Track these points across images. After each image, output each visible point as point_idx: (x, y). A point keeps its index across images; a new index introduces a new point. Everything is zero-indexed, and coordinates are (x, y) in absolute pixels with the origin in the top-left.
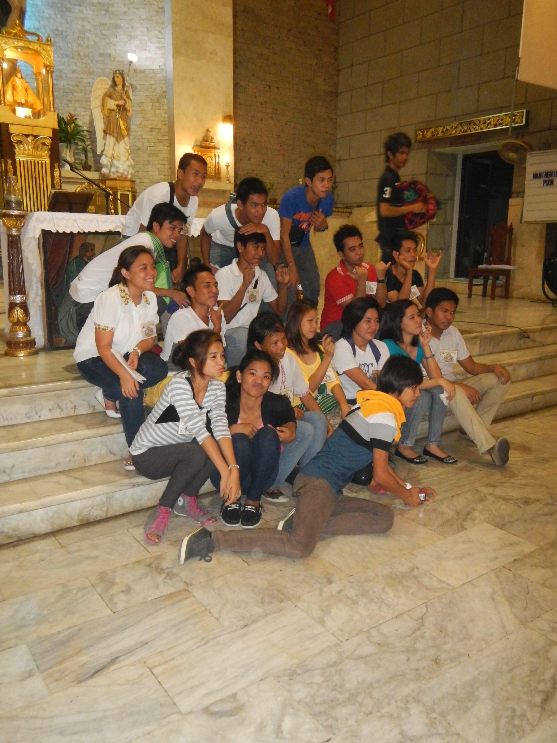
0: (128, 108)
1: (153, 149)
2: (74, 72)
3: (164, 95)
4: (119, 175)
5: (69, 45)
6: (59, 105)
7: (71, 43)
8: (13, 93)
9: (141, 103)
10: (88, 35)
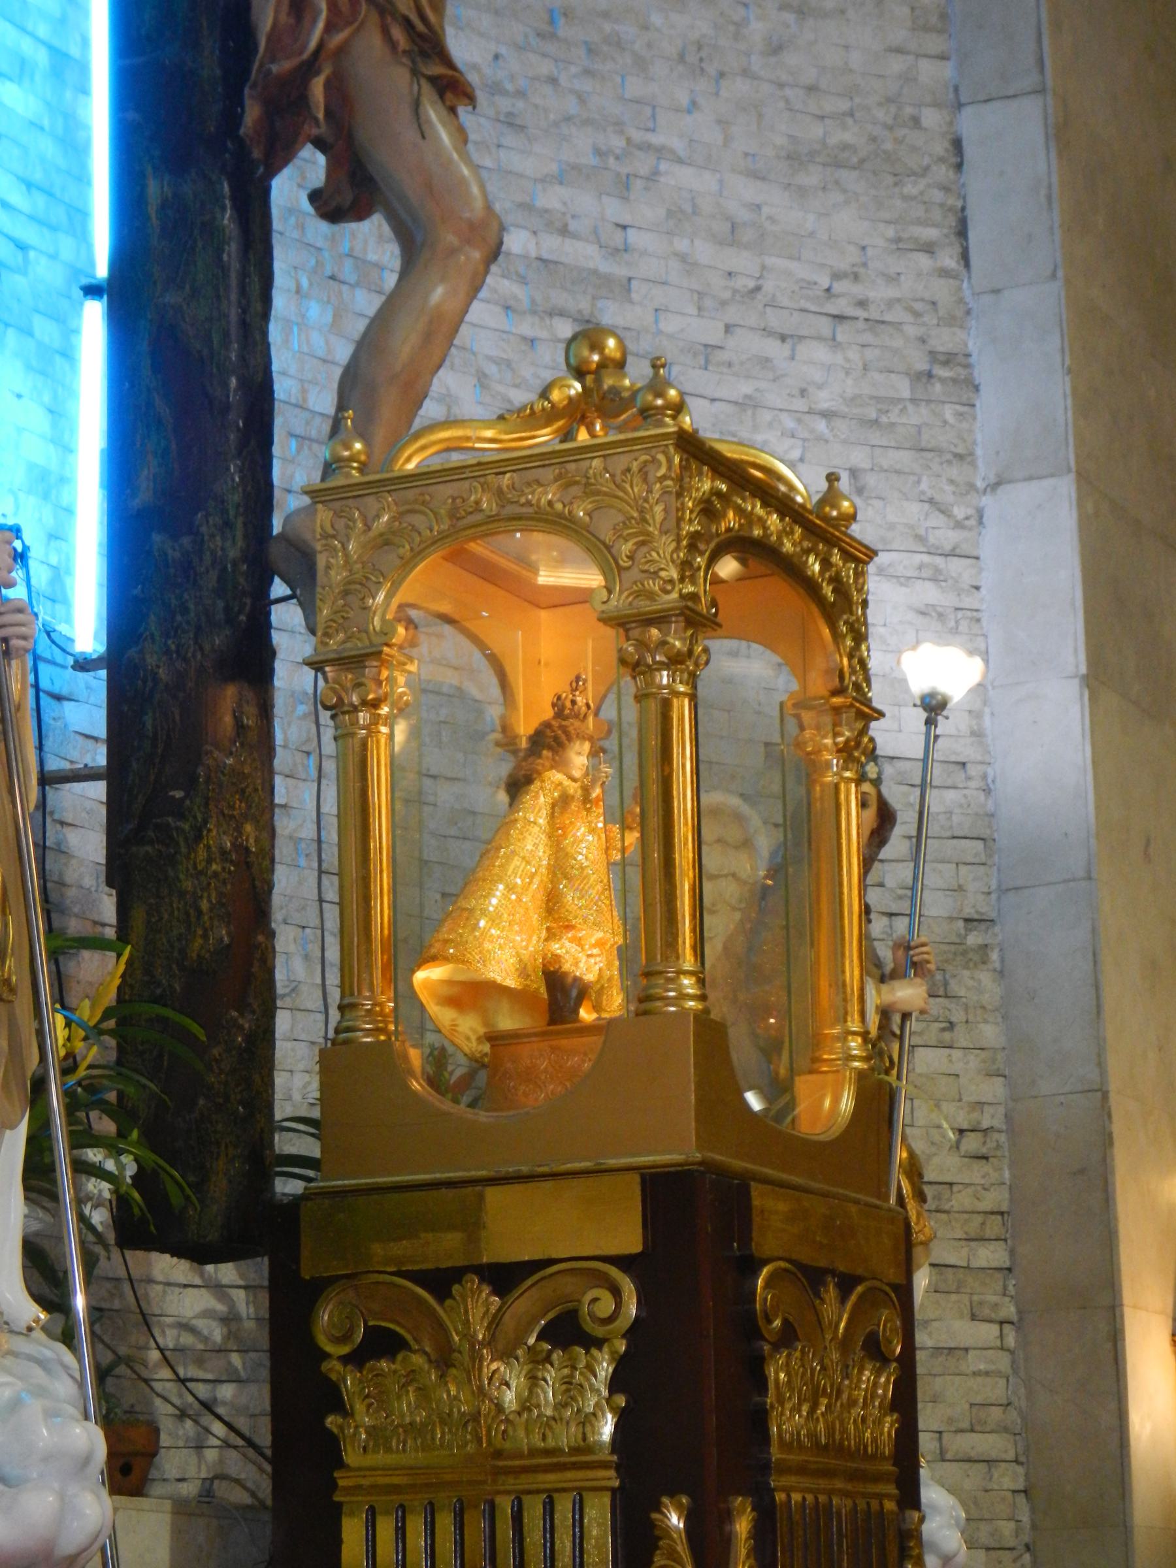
3: (973, 939)
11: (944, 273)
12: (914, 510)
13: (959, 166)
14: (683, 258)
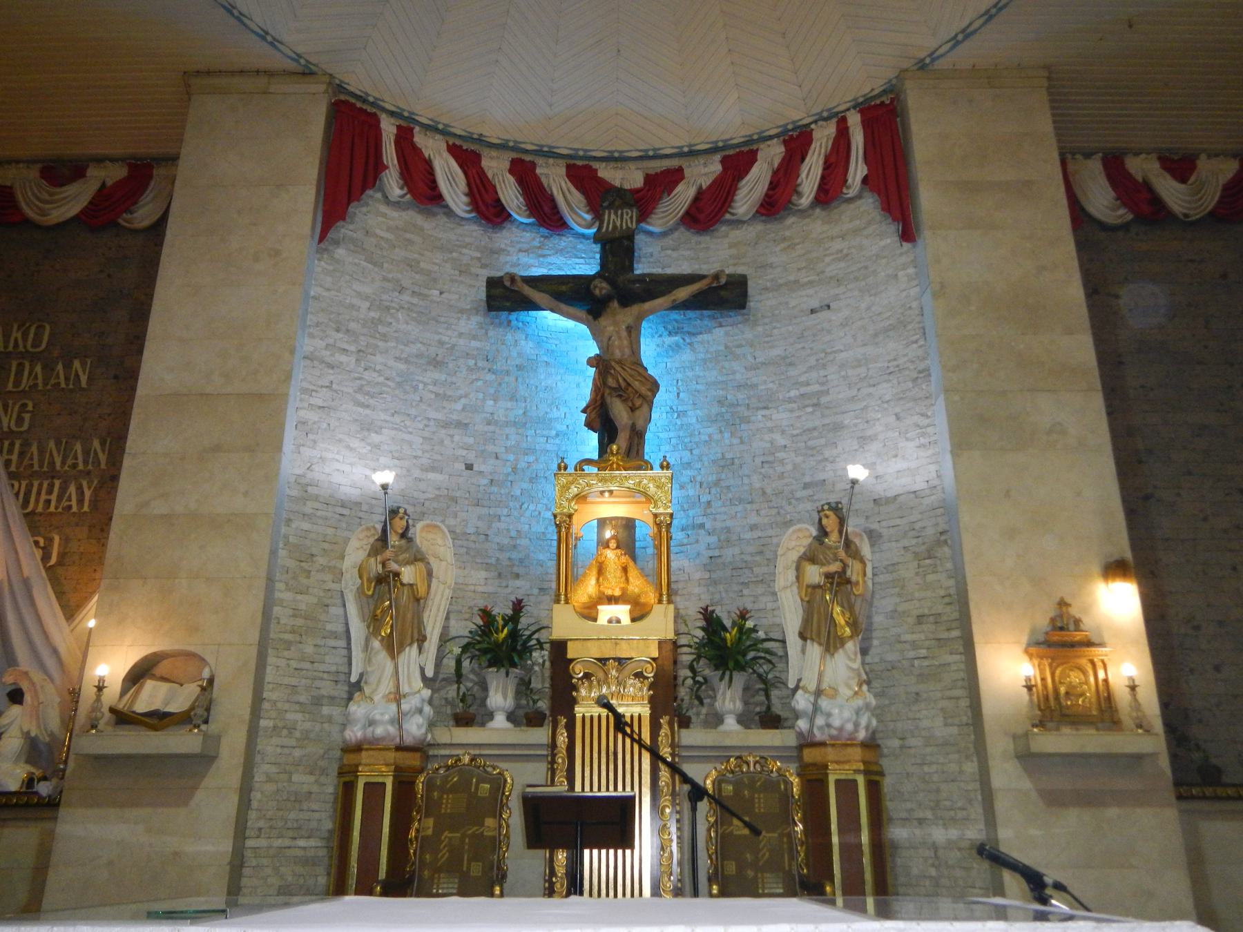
0: (854, 579)
1: (926, 663)
2: (753, 527)
3: (943, 538)
4: (834, 732)
5: (746, 481)
6: (724, 595)
7: (748, 476)
8: (598, 580)
9: (894, 565)
10: (781, 455)
11: (921, 346)
12: (916, 419)
13: (922, 315)
14: (843, 377)
